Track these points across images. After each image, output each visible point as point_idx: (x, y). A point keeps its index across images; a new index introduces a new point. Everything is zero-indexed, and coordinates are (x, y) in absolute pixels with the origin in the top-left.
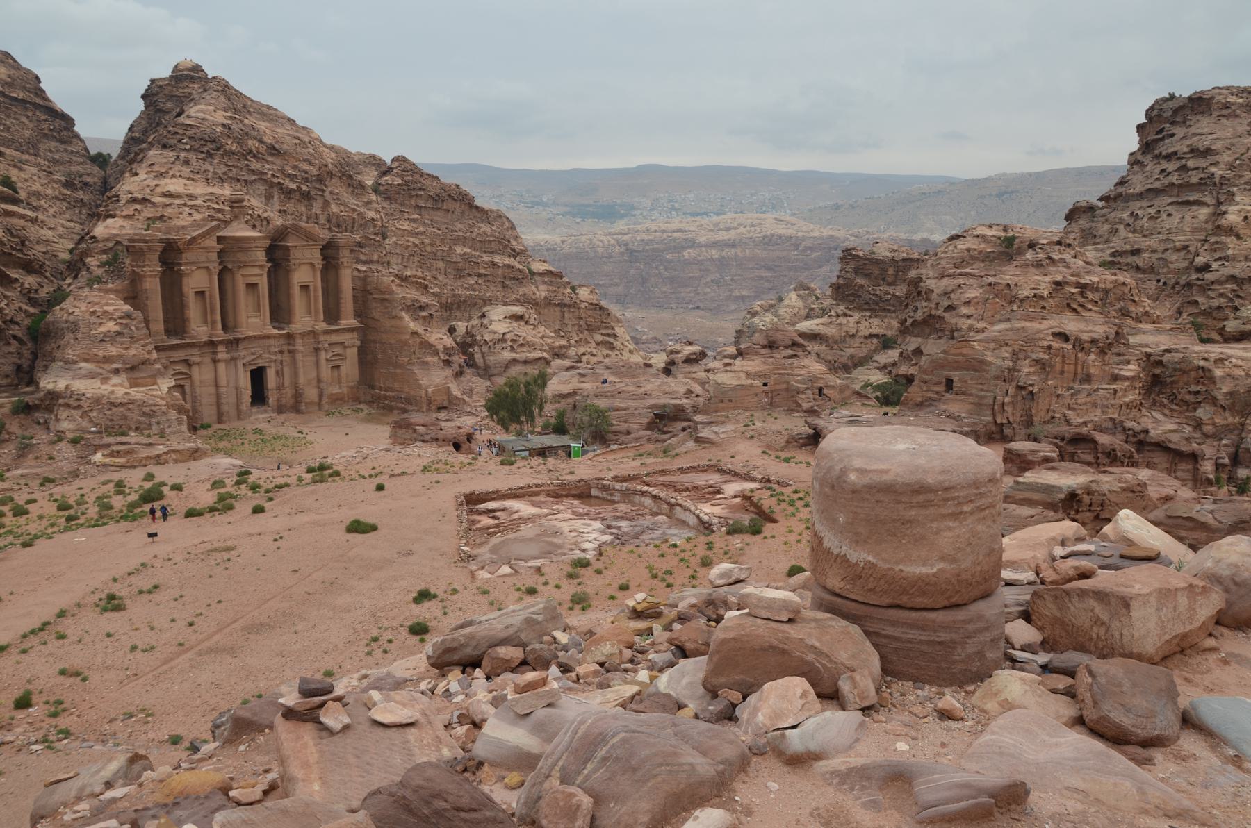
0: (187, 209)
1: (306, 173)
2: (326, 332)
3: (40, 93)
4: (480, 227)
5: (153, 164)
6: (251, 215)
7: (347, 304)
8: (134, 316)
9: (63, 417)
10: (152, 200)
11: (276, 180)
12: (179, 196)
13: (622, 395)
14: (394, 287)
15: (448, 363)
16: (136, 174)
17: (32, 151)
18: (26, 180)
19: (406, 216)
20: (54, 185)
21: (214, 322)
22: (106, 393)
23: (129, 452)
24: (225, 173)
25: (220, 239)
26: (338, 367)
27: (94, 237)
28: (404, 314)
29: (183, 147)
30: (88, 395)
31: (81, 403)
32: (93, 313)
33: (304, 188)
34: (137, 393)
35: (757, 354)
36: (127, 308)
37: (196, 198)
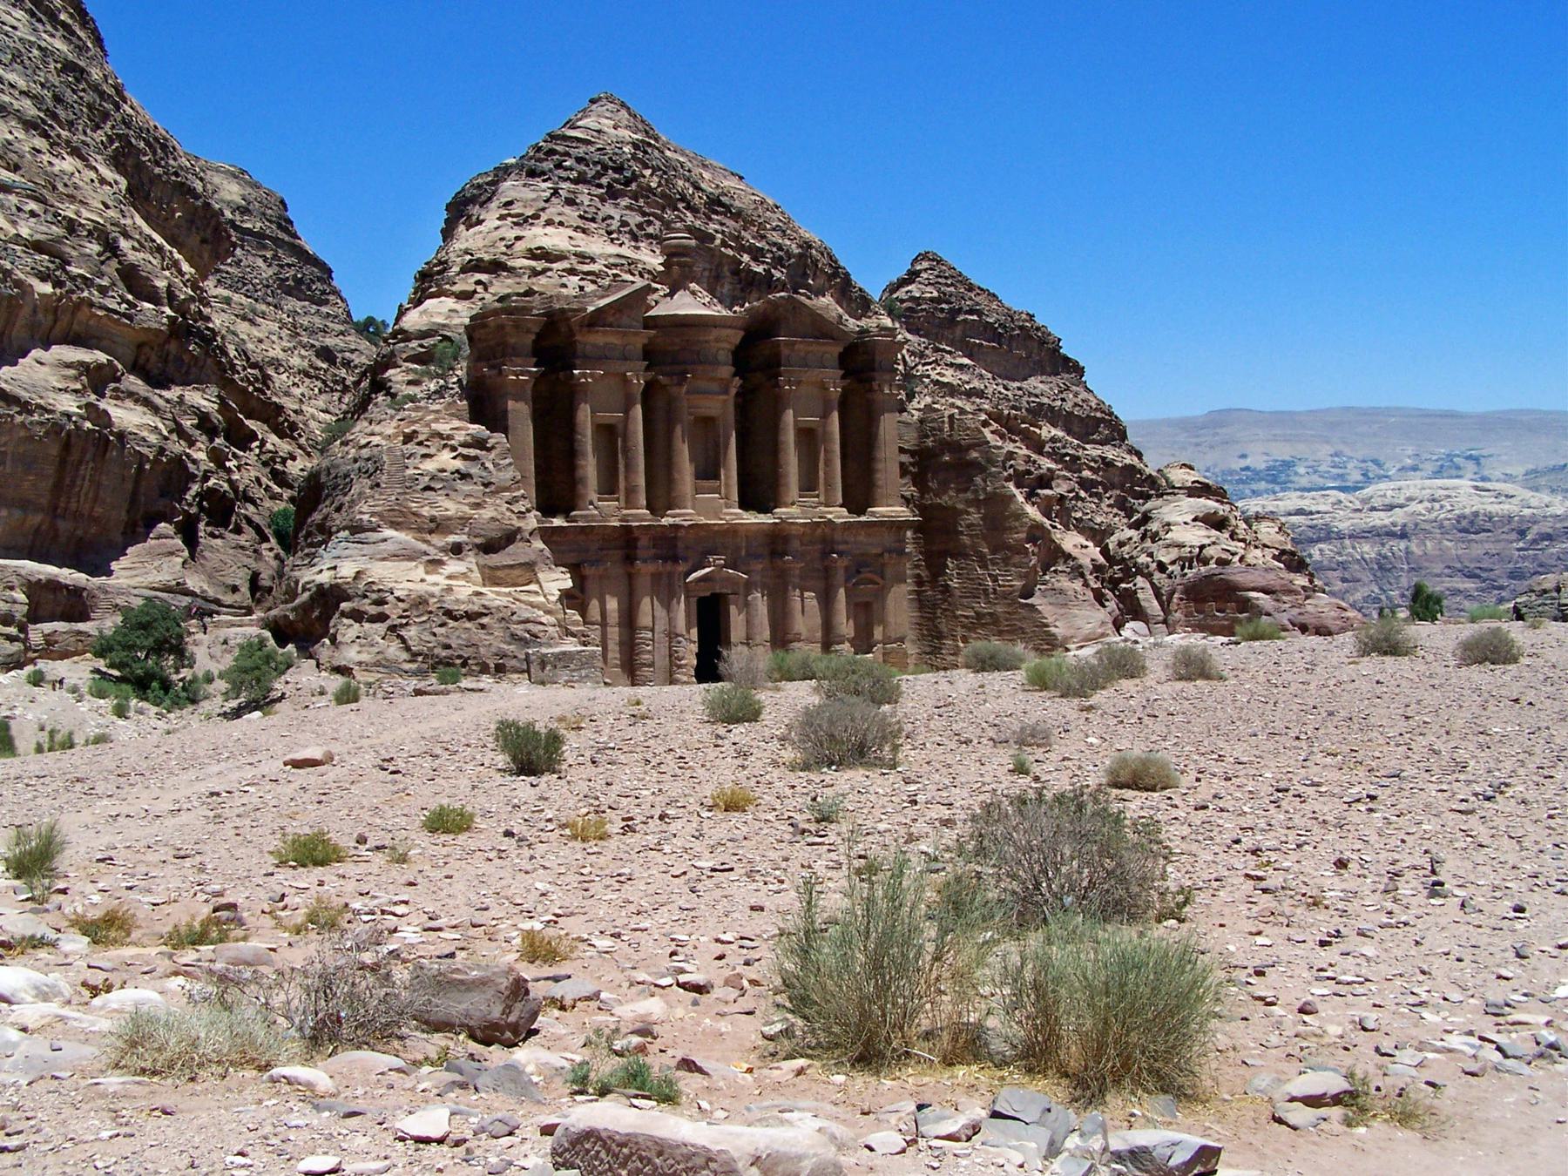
1: (780, 248)
2: (847, 526)
3: (285, 224)
4: (1076, 395)
5: (509, 204)
8: (491, 442)
9: (347, 639)
12: (561, 257)
14: (986, 431)
16: (480, 222)
17: (270, 299)
18: (260, 341)
19: (948, 358)
20: (303, 352)
21: (631, 491)
22: (436, 590)
24: (640, 226)
27: (402, 331)
28: (1011, 485)
29: (564, 174)
30: (397, 593)
31: (386, 609)
32: (408, 438)
36: (477, 429)
37: (593, 260)
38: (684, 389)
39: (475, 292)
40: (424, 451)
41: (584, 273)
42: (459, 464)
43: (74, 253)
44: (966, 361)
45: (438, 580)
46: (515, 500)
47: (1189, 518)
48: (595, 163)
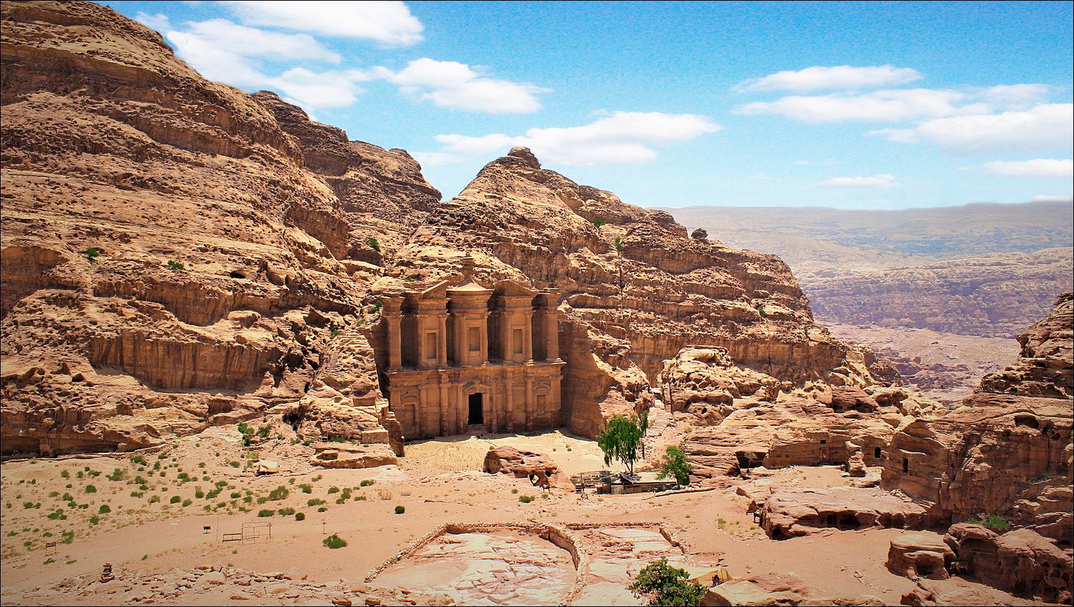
0: (436, 269)
3: (419, 177)
6: (489, 273)
7: (553, 346)
10: (414, 263)
11: (518, 244)
12: (433, 260)
13: (715, 442)
14: (589, 332)
15: (630, 399)
18: (388, 241)
21: (441, 357)
22: (335, 409)
23: (335, 456)
24: (474, 241)
25: (449, 294)
26: (544, 396)
33: (544, 249)
34: (356, 411)
35: (819, 412)
36: (367, 347)
38: (465, 318)
39: (400, 274)
40: (345, 355)
41: (441, 267)
42: (355, 361)
43: (247, 273)
44: (653, 268)
45: (338, 404)
46: (372, 374)
47: (691, 359)
48: (458, 216)
